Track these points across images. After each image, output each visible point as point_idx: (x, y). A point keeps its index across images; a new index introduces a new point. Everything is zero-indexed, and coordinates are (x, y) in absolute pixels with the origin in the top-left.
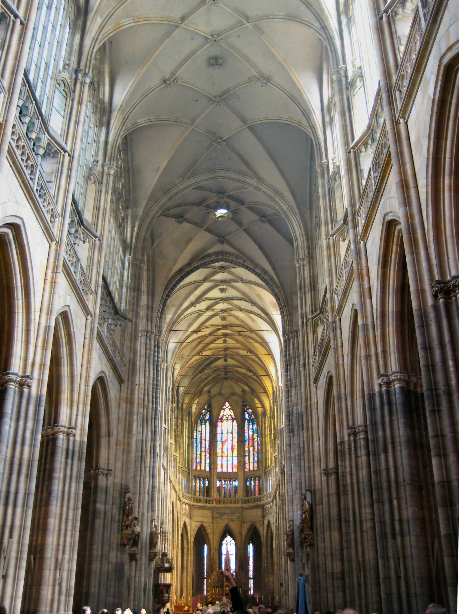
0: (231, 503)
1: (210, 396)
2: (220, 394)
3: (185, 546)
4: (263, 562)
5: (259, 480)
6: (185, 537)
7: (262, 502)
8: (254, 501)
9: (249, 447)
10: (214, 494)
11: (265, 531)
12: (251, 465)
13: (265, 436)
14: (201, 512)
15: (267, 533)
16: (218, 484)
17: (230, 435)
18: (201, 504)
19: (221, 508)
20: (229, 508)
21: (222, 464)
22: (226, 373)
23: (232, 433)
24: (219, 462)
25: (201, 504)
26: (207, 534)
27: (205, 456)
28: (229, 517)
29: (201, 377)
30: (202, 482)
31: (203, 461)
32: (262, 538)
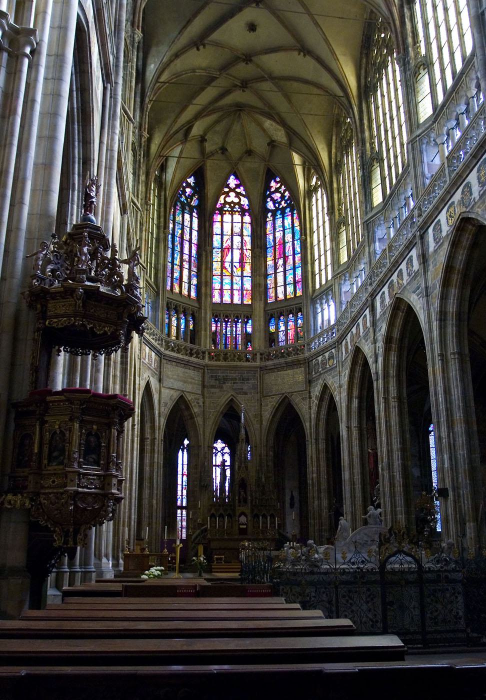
0: (240, 359)
1: (202, 151)
2: (224, 150)
3: (148, 435)
4: (309, 470)
5: (296, 316)
6: (147, 418)
7: (307, 354)
8: (289, 354)
9: (275, 259)
10: (206, 344)
11: (314, 409)
12: (280, 290)
13: (312, 232)
14: (180, 370)
15: (318, 413)
16: (214, 328)
17: (237, 239)
18: (180, 356)
19: (220, 366)
20: (236, 367)
21: (221, 290)
22: (244, 85)
23: (242, 235)
24: (217, 285)
25: (180, 356)
26: (192, 417)
27: (190, 269)
28: (235, 386)
29: (194, 71)
30: (183, 321)
31: (185, 278)
32: (308, 424)
